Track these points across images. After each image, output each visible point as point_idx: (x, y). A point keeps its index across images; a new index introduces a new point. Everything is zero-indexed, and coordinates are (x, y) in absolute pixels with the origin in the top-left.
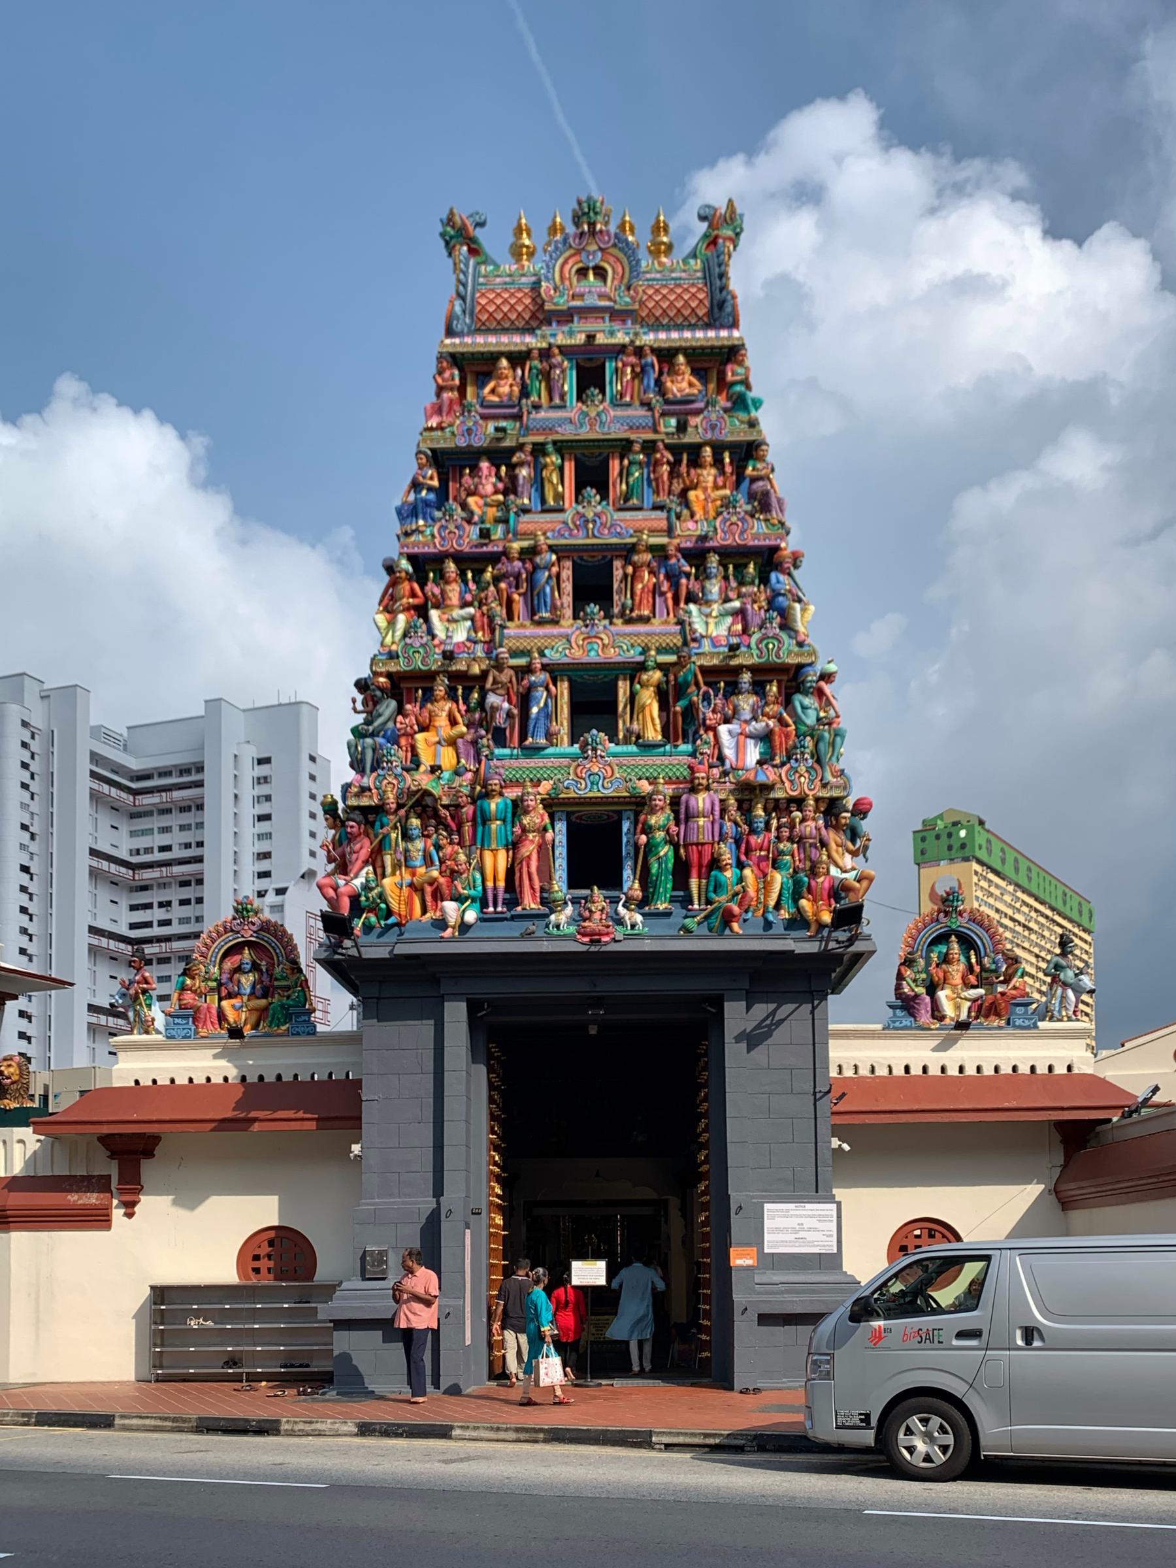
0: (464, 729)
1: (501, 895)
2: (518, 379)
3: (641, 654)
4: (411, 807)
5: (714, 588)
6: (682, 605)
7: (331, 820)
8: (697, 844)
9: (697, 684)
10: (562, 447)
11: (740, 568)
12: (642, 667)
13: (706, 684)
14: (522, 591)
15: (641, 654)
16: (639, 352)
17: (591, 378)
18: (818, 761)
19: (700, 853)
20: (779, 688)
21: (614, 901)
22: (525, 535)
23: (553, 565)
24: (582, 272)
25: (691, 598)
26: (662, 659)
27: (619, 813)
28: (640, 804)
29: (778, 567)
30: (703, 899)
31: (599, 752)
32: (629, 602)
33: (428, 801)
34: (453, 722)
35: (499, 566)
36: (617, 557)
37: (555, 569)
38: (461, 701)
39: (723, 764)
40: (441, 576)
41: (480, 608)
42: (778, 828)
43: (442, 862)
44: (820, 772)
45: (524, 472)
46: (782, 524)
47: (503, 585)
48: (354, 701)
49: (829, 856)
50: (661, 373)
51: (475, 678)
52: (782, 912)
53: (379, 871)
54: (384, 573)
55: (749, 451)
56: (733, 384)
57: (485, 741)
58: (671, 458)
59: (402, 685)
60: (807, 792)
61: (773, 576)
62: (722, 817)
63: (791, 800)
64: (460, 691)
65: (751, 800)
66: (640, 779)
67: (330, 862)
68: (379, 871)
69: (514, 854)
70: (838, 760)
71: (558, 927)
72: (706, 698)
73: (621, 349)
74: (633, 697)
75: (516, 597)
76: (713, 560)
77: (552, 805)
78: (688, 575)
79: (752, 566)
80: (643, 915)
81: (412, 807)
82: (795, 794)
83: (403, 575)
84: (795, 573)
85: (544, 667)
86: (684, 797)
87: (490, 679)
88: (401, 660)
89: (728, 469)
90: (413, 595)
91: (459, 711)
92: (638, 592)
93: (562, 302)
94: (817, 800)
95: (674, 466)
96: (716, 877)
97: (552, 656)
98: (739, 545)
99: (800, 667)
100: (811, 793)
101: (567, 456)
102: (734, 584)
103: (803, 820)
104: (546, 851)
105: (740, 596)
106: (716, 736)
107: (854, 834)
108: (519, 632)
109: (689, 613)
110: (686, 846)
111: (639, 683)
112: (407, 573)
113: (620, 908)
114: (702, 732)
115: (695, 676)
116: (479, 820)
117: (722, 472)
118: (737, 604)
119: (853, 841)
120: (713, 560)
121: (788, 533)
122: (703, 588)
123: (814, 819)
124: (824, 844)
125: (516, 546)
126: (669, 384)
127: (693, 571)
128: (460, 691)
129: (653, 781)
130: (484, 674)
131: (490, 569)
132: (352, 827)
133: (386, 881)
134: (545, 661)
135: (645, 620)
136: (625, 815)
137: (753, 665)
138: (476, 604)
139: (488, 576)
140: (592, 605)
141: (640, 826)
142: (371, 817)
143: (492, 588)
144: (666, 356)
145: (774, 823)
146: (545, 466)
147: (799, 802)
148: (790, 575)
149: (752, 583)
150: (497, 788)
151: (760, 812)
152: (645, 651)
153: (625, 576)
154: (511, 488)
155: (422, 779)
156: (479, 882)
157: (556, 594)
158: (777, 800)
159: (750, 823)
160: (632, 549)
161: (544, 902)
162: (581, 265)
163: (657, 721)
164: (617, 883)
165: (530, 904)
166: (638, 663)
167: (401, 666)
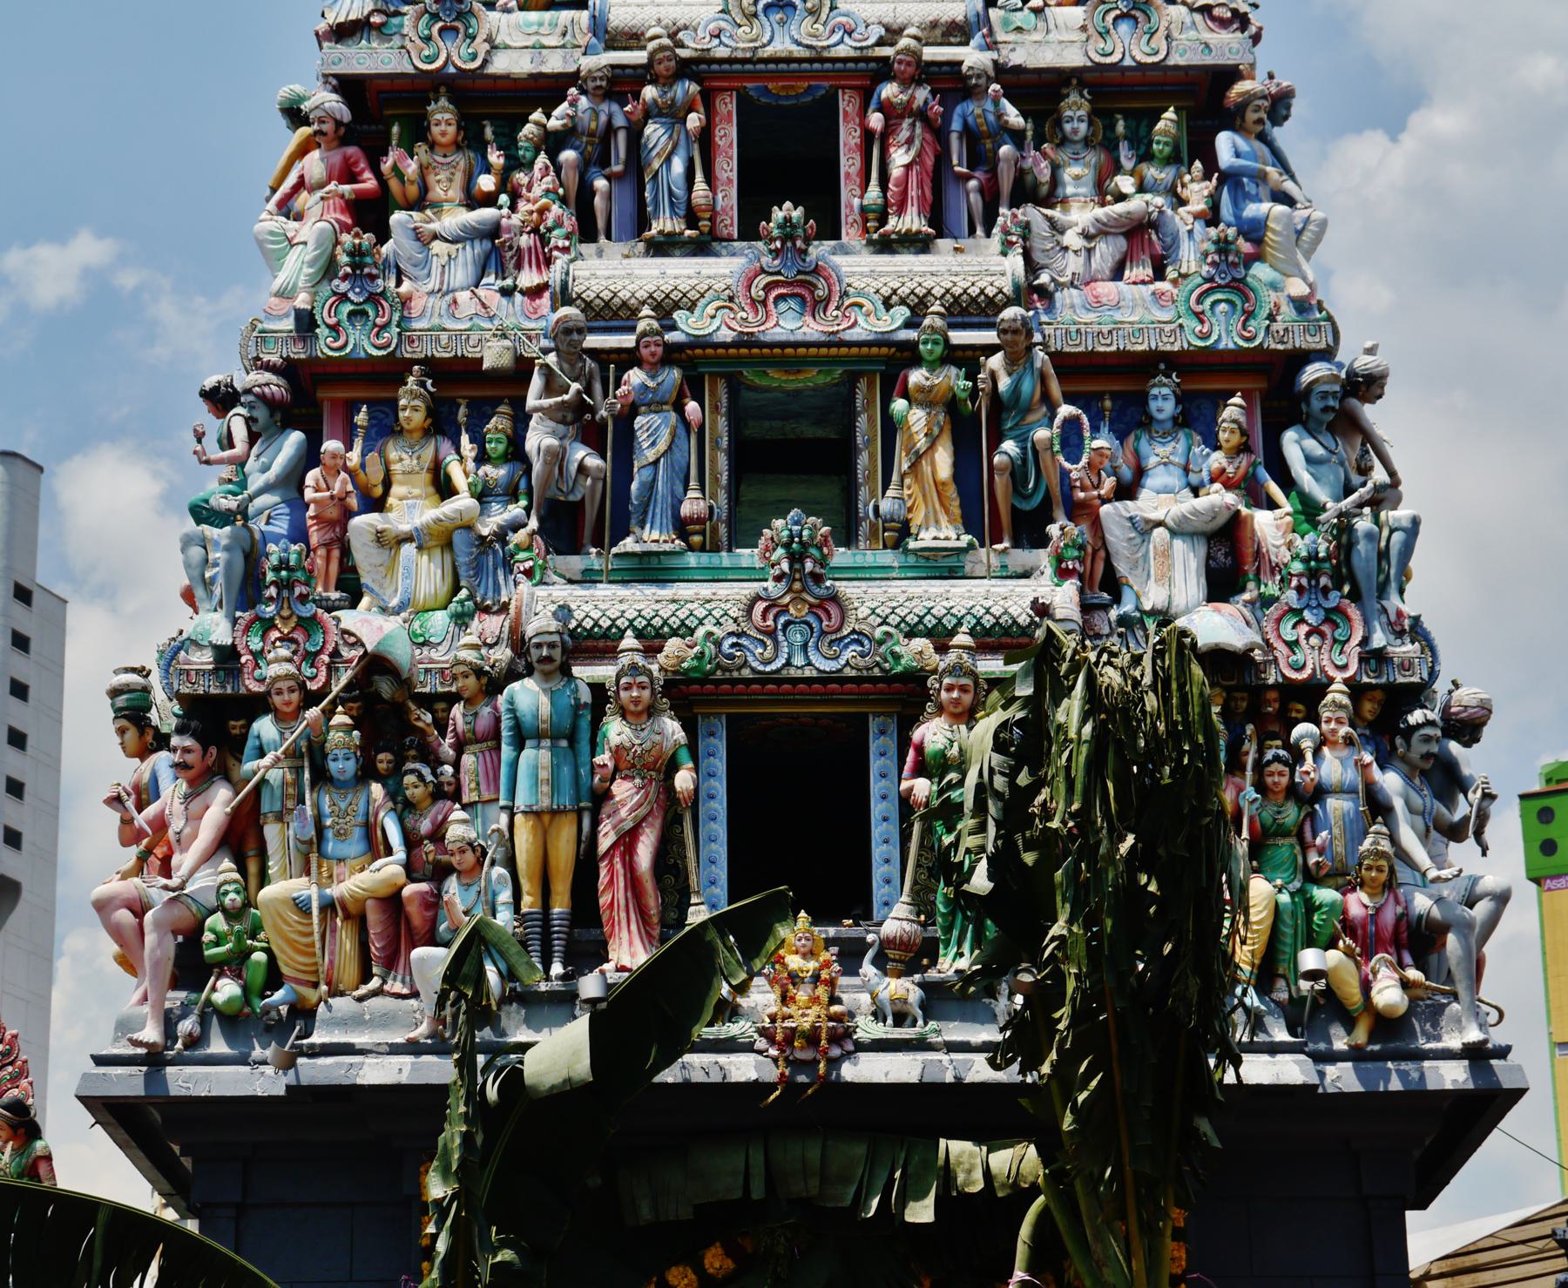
0: (473, 502)
3: (908, 325)
4: (334, 703)
5: (1076, 175)
6: (1002, 210)
7: (132, 734)
9: (1046, 398)
12: (909, 355)
13: (1069, 399)
14: (617, 168)
15: (908, 325)
20: (1248, 410)
23: (690, 110)
25: (1025, 192)
26: (959, 337)
28: (907, 695)
29: (1233, 119)
31: (809, 565)
33: (385, 687)
34: (444, 488)
35: (563, 108)
36: (844, 88)
37: (694, 121)
39: (1117, 599)
40: (417, 132)
41: (513, 208)
42: (1259, 766)
43: (411, 841)
46: (1240, 20)
47: (568, 155)
48: (199, 437)
49: (1393, 839)
51: (496, 376)
52: (1281, 983)
53: (253, 868)
54: (282, 122)
57: (519, 537)
59: (321, 394)
60: (1332, 672)
61: (1226, 144)
63: (1289, 690)
64: (462, 411)
66: (910, 635)
67: (125, 843)
68: (253, 868)
70: (1401, 592)
72: (1071, 438)
74: (891, 428)
75: (601, 184)
77: (687, 694)
78: (1017, 137)
79: (1170, 114)
80: (920, 985)
84: (1282, 135)
85: (672, 355)
87: (537, 382)
88: (322, 331)
90: (348, 175)
92: (896, 172)
94: (1356, 690)
97: (688, 325)
99: (1303, 357)
100: (1339, 676)
102: (1126, 157)
103: (1322, 742)
104: (673, 815)
105: (1141, 188)
106: (1097, 525)
107: (1445, 779)
108: (613, 270)
109: (1027, 226)
111: (905, 394)
112: (338, 123)
113: (868, 969)
114: (1062, 520)
115: (1043, 378)
116: (505, 734)
118: (1136, 204)
119: (1450, 803)
121: (1256, 39)
122: (1056, 168)
123: (1349, 741)
124: (1377, 807)
127: (1029, 126)
128: (462, 411)
129: (941, 637)
130: (523, 368)
131: (537, 115)
132: (186, 750)
133: (267, 893)
135: (918, 244)
136: (873, 726)
137: (1182, 353)
138: (504, 199)
139: (528, 130)
140: (788, 204)
141: (911, 753)
142: (235, 725)
143: (542, 159)
145: (1251, 748)
147: (1309, 694)
148: (1263, 138)
149: (1174, 159)
150: (557, 653)
153: (868, 135)
155: (368, 625)
156: (505, 896)
157: (699, 177)
160: (883, 70)
163: (952, 491)
164: (860, 905)
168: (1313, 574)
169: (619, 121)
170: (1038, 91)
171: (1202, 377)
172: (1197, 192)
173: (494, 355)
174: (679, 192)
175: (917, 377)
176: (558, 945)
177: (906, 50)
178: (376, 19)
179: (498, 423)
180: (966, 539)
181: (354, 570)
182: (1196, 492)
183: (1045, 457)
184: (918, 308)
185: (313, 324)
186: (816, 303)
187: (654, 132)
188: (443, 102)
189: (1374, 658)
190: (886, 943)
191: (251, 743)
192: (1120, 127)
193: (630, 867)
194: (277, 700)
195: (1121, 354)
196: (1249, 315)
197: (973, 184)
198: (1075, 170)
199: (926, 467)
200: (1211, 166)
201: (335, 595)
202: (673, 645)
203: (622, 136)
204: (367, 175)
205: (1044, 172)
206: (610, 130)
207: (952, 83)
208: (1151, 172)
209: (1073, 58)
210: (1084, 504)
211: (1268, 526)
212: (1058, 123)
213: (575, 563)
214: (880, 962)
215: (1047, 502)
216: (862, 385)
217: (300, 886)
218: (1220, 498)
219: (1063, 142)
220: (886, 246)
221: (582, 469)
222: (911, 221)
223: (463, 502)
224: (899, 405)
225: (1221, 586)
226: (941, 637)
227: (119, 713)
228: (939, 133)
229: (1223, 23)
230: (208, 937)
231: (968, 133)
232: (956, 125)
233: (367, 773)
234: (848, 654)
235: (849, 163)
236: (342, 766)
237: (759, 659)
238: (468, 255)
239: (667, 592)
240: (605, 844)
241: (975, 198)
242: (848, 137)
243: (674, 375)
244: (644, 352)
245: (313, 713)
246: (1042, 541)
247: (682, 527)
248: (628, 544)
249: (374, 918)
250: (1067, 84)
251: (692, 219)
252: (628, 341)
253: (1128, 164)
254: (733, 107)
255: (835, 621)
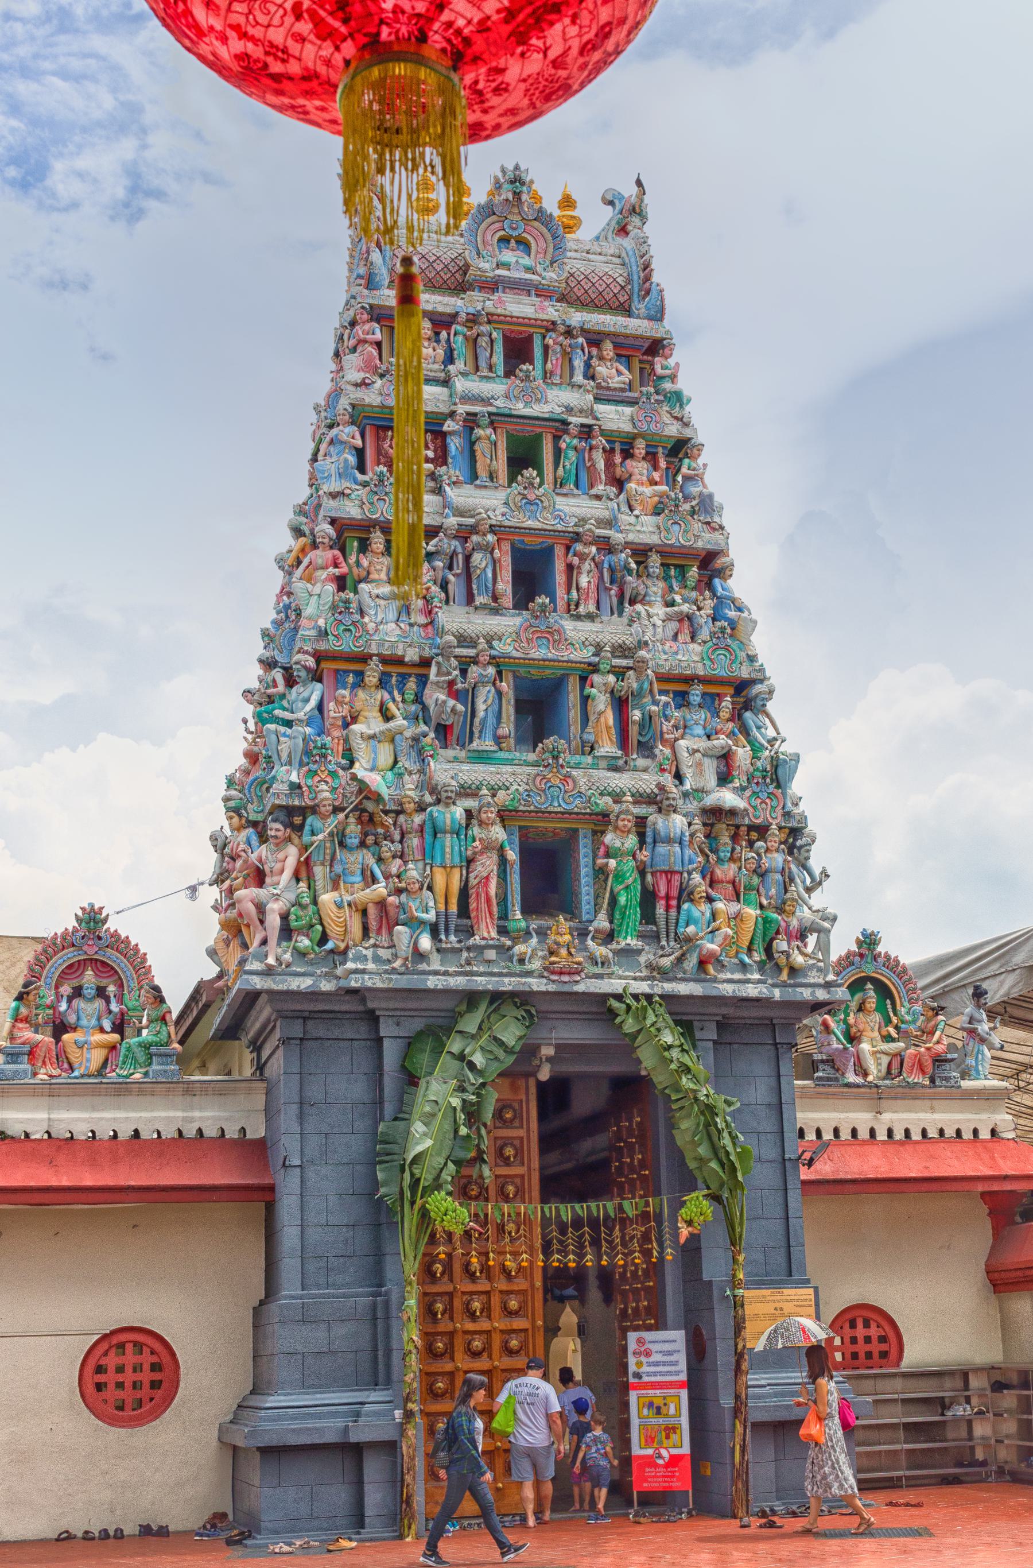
1: (454, 921)
2: (443, 342)
8: (666, 872)
10: (496, 420)
11: (682, 569)
13: (662, 692)
16: (569, 333)
17: (518, 350)
18: (779, 786)
19: (669, 882)
21: (583, 934)
22: (460, 513)
24: (504, 240)
27: (576, 831)
30: (672, 935)
32: (574, 594)
33: (370, 806)
38: (396, 693)
39: (681, 783)
44: (780, 796)
45: (454, 444)
46: (722, 528)
50: (590, 357)
55: (680, 449)
56: (661, 378)
57: (428, 740)
58: (608, 447)
62: (691, 842)
63: (751, 828)
65: (712, 825)
66: (601, 794)
69: (468, 873)
71: (521, 961)
73: (551, 326)
74: (585, 699)
75: (451, 578)
76: (655, 561)
81: (352, 811)
82: (758, 821)
83: (326, 541)
86: (651, 818)
89: (663, 464)
91: (394, 700)
93: (485, 266)
95: (609, 453)
96: (688, 910)
98: (684, 546)
101: (499, 431)
103: (767, 850)
106: (673, 749)
110: (653, 874)
112: (331, 539)
113: (589, 942)
115: (651, 684)
117: (656, 467)
120: (655, 561)
125: (452, 521)
126: (599, 369)
130: (425, 663)
132: (277, 830)
134: (494, 653)
135: (591, 617)
136: (581, 833)
144: (595, 339)
146: (479, 439)
147: (762, 830)
151: (725, 839)
152: (599, 648)
154: (442, 458)
156: (431, 904)
158: (737, 827)
159: (715, 851)
161: (503, 931)
162: (502, 233)
163: (613, 731)
165: (487, 931)
166: (590, 664)
167: (331, 644)
168: (764, 778)
169: (459, 550)
170: (641, 553)
171: (714, 688)
172: (709, 604)
173: (412, 655)
174: (490, 586)
175: (596, 678)
176: (452, 927)
177: (590, 530)
178: (347, 491)
179: (412, 685)
180: (620, 753)
181: (350, 750)
182: (709, 737)
183: (656, 719)
184: (599, 648)
185: (326, 634)
186: (555, 641)
187: (477, 558)
188: (378, 533)
189: (787, 815)
190: (597, 931)
191: (307, 828)
192: (672, 572)
193: (487, 894)
194: (323, 809)
195: (681, 675)
196: (732, 662)
197: (613, 592)
198: (655, 589)
199: (602, 720)
200: (714, 594)
201: (344, 762)
202: (501, 794)
203: (460, 556)
204: (344, 564)
205: (642, 589)
206: (455, 553)
207: (606, 546)
208: (686, 592)
209: (654, 539)
210: (667, 741)
211: (742, 754)
212: (646, 567)
213: (450, 753)
214: (593, 939)
215: (653, 738)
216: (571, 679)
217: (335, 895)
218: (722, 741)
219: (648, 576)
220: (578, 618)
221: (453, 710)
222: (592, 608)
223: (400, 722)
224: (588, 690)
225: (724, 779)
226: (617, 797)
227: (228, 809)
228: (598, 565)
229: (714, 529)
230: (292, 917)
231: (612, 570)
232: (606, 565)
233: (363, 844)
234: (577, 802)
235: (560, 578)
236: (353, 841)
237: (539, 801)
238: (395, 605)
239: (492, 769)
240: (473, 882)
241: (615, 600)
242: (559, 566)
243: (491, 671)
244: (481, 659)
245: (341, 816)
246: (652, 756)
247: (498, 740)
248: (475, 745)
249: (372, 911)
250: (651, 550)
251: (495, 598)
252: (472, 652)
253: (676, 589)
254: (509, 548)
255: (571, 787)
